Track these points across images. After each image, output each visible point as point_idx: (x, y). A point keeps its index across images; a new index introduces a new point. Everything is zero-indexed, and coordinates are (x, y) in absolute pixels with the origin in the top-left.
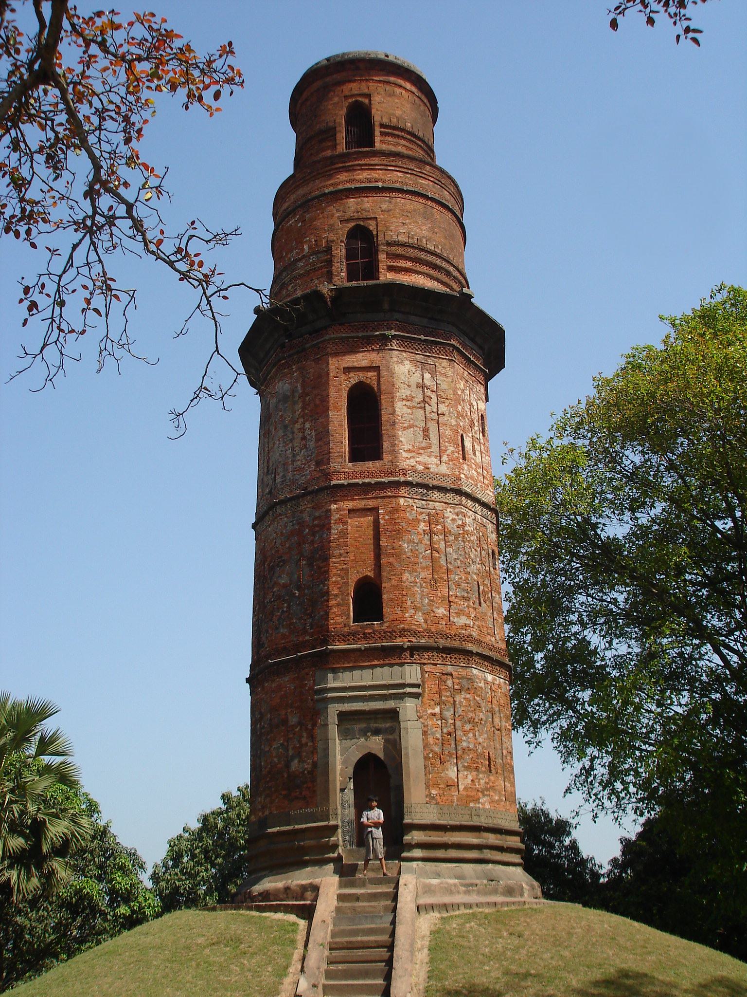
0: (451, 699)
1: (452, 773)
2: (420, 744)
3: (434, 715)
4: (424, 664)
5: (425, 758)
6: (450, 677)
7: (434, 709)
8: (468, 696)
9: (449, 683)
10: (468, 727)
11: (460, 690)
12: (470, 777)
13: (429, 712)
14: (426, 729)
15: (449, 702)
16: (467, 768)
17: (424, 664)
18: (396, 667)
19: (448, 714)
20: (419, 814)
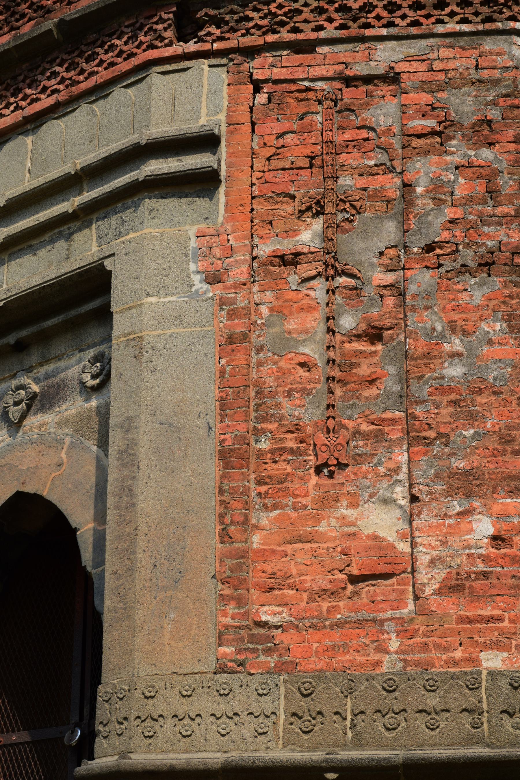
0: (391, 184)
1: (382, 522)
2: (202, 392)
3: (290, 260)
4: (250, 52)
5: (225, 456)
6: (384, 89)
7: (291, 233)
8: (487, 154)
9: (384, 112)
10: (476, 292)
11: (441, 135)
12: (484, 527)
13: (265, 250)
14: (240, 326)
15: (378, 195)
16: (467, 485)
17: (250, 52)
18: (118, 93)
19: (369, 244)
20: (167, 729)
